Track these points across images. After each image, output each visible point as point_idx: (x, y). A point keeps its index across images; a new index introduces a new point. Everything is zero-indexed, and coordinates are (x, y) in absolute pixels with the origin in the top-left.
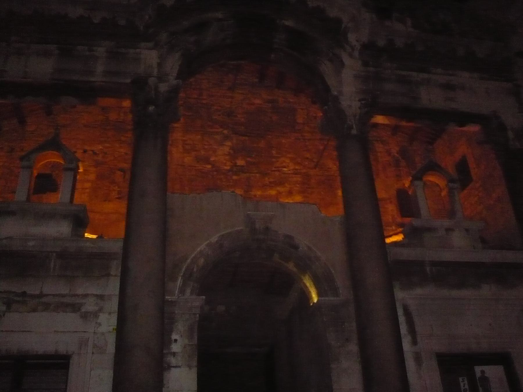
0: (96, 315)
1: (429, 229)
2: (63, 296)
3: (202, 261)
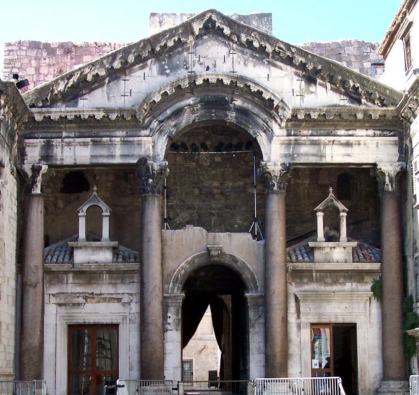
0: (129, 303)
1: (320, 248)
2: (112, 294)
3: (183, 271)
